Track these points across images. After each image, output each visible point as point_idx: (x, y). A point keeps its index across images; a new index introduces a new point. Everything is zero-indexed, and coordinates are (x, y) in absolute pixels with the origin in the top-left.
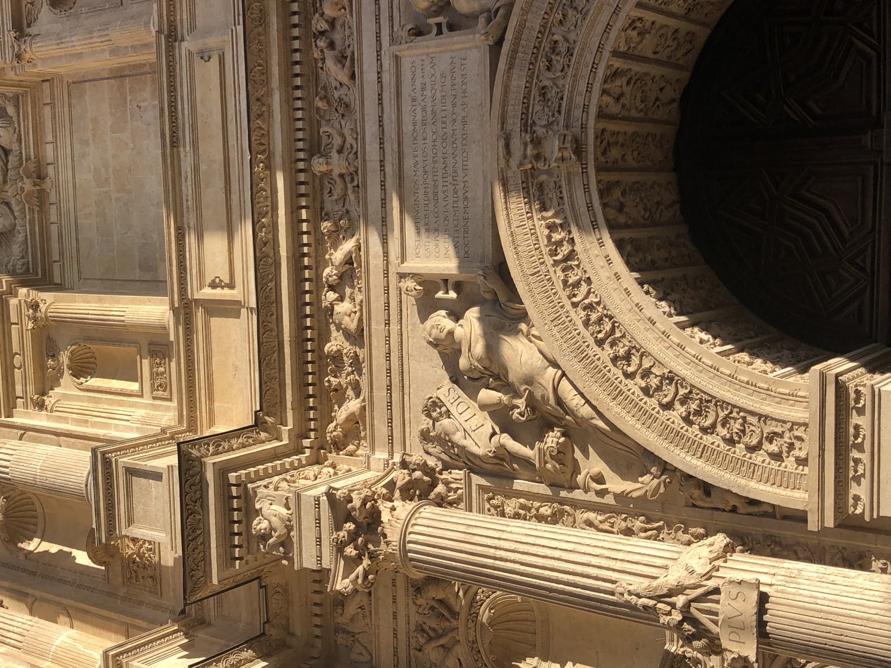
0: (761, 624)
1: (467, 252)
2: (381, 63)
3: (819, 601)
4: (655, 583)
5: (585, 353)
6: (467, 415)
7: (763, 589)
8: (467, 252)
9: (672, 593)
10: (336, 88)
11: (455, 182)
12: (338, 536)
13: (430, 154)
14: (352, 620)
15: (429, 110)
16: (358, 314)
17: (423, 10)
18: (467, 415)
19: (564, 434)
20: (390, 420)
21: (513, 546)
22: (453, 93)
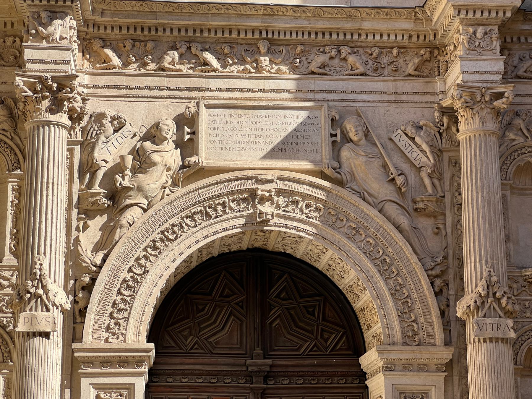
0: (35, 334)
1: (211, 149)
2: (319, 93)
3: (49, 360)
4: (48, 278)
5: (156, 224)
6: (116, 143)
7: (51, 333)
8: (211, 149)
9: (43, 287)
10: (307, 59)
11: (250, 142)
12: (49, 79)
13: (266, 127)
16: (173, 67)
17: (345, 125)
18: (116, 143)
19: (108, 205)
20: (108, 87)
21: (55, 194)
22: (299, 144)
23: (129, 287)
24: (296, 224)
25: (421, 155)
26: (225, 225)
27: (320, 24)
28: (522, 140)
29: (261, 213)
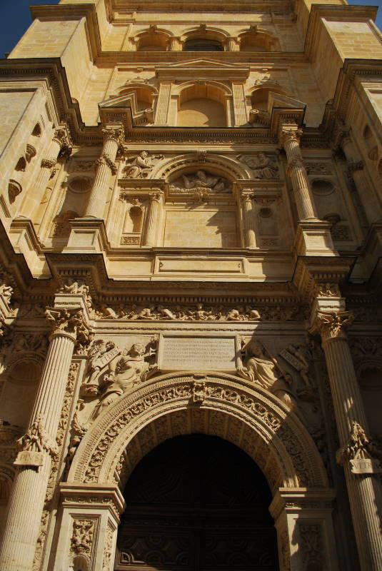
14: (36, 311)
15: (216, 348)
20: (107, 328)
23: (104, 445)
24: (220, 404)
25: (300, 363)
26: (172, 405)
27: (233, 293)
28: (362, 355)
29: (196, 397)
